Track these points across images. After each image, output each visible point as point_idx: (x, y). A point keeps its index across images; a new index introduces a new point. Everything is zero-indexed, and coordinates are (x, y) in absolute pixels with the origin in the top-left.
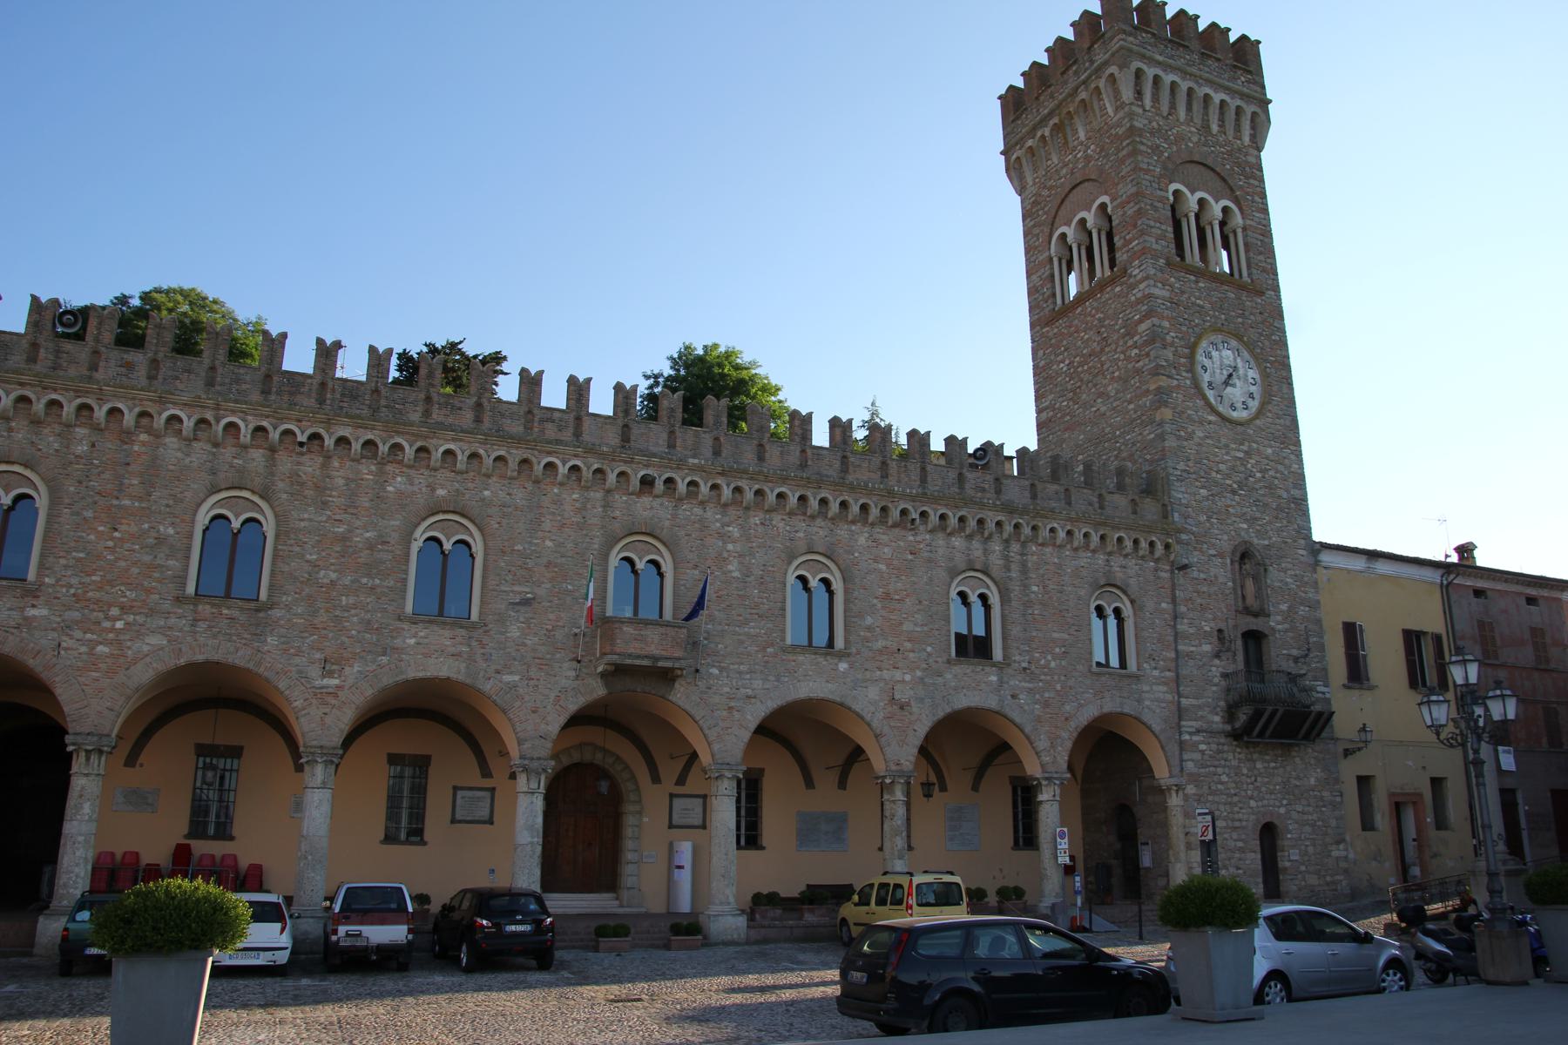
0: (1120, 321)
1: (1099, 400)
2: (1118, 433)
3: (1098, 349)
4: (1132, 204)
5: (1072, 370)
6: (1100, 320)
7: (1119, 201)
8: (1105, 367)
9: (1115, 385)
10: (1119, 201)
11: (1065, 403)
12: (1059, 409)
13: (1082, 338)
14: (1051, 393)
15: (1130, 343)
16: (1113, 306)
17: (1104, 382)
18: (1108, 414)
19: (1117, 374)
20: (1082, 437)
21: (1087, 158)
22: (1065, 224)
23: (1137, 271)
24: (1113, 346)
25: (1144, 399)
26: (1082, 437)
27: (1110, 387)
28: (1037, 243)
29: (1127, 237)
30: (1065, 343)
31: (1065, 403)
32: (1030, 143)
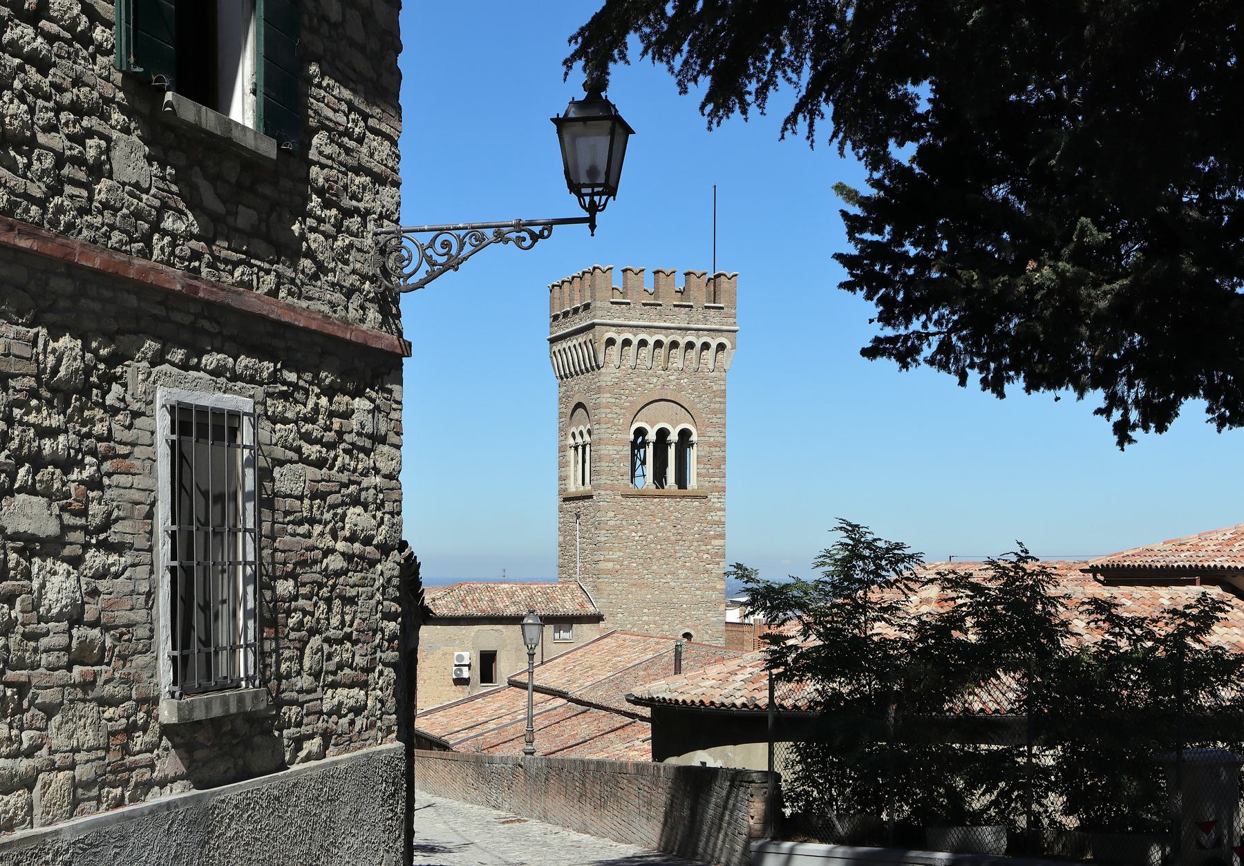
0: (695, 529)
1: (669, 576)
2: (685, 606)
3: (673, 538)
4: (718, 449)
5: (644, 543)
6: (677, 518)
7: (707, 439)
8: (678, 555)
9: (685, 571)
10: (707, 439)
11: (635, 565)
12: (628, 567)
13: (658, 523)
14: (620, 551)
15: (703, 548)
16: (691, 514)
17: (676, 565)
18: (677, 589)
19: (687, 564)
20: (648, 596)
21: (680, 389)
22: (647, 422)
23: (717, 500)
24: (687, 544)
25: (711, 592)
26: (648, 596)
27: (680, 572)
28: (616, 421)
29: (710, 471)
30: (639, 518)
31: (635, 565)
32: (630, 336)
